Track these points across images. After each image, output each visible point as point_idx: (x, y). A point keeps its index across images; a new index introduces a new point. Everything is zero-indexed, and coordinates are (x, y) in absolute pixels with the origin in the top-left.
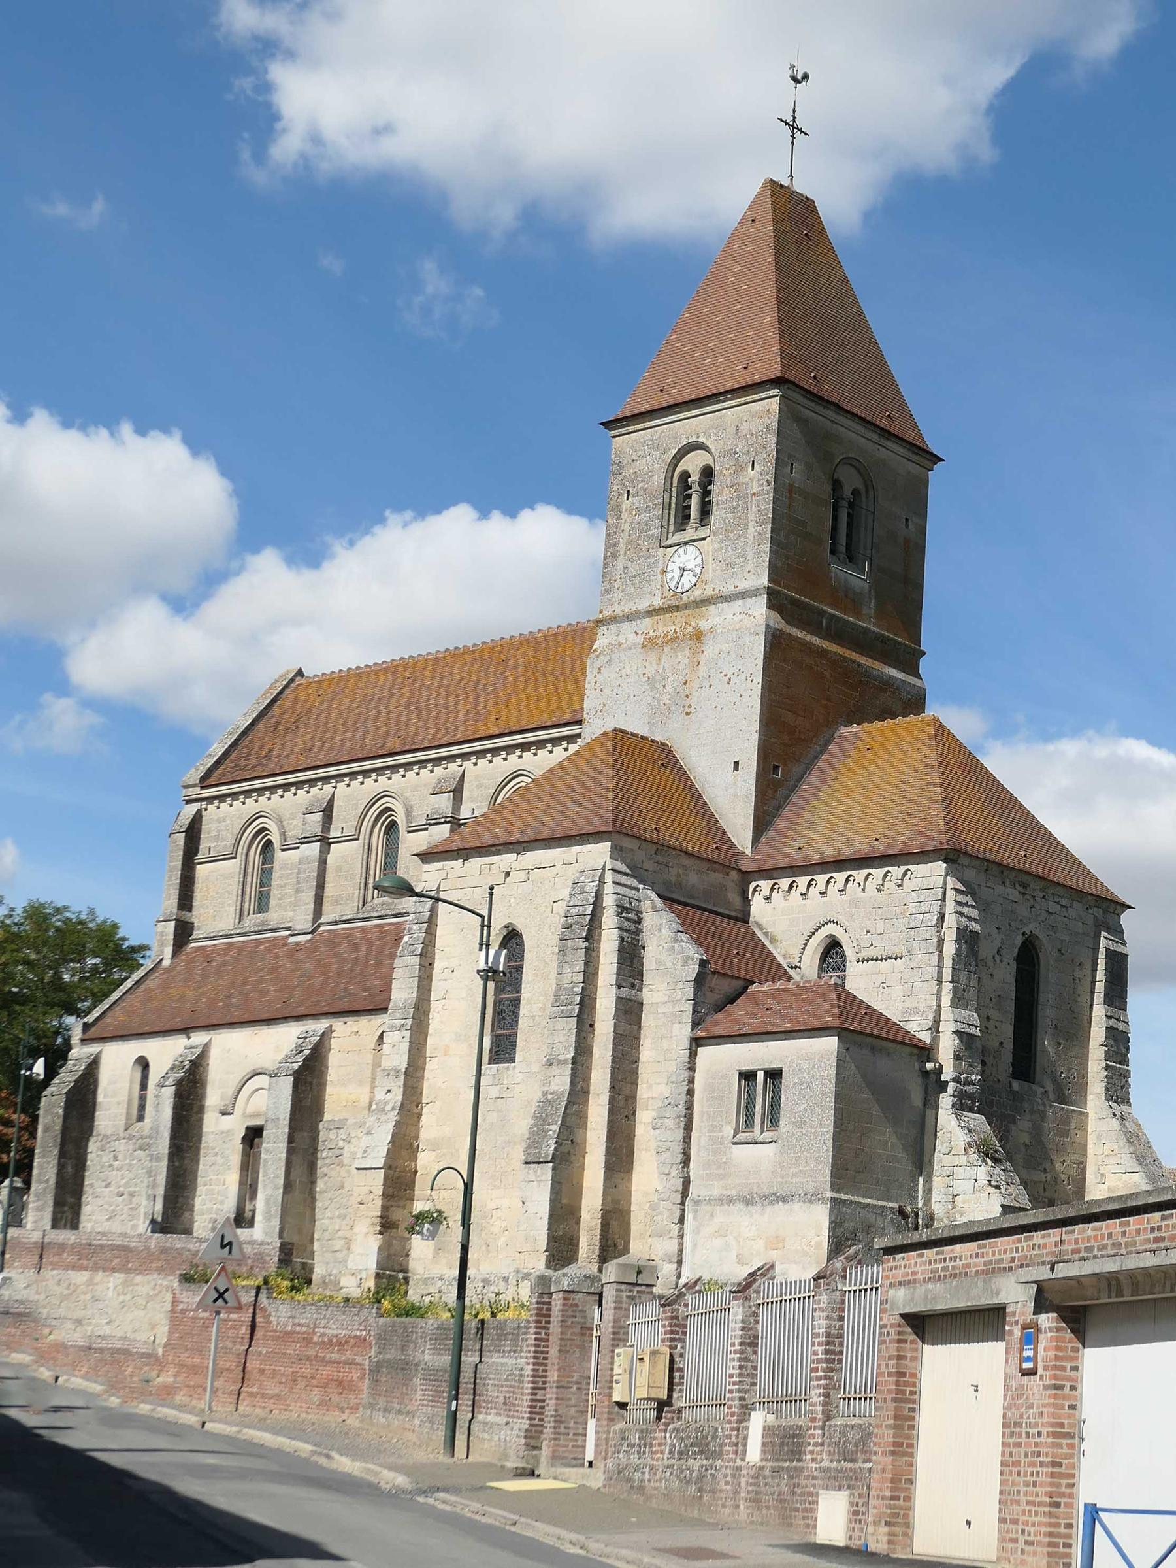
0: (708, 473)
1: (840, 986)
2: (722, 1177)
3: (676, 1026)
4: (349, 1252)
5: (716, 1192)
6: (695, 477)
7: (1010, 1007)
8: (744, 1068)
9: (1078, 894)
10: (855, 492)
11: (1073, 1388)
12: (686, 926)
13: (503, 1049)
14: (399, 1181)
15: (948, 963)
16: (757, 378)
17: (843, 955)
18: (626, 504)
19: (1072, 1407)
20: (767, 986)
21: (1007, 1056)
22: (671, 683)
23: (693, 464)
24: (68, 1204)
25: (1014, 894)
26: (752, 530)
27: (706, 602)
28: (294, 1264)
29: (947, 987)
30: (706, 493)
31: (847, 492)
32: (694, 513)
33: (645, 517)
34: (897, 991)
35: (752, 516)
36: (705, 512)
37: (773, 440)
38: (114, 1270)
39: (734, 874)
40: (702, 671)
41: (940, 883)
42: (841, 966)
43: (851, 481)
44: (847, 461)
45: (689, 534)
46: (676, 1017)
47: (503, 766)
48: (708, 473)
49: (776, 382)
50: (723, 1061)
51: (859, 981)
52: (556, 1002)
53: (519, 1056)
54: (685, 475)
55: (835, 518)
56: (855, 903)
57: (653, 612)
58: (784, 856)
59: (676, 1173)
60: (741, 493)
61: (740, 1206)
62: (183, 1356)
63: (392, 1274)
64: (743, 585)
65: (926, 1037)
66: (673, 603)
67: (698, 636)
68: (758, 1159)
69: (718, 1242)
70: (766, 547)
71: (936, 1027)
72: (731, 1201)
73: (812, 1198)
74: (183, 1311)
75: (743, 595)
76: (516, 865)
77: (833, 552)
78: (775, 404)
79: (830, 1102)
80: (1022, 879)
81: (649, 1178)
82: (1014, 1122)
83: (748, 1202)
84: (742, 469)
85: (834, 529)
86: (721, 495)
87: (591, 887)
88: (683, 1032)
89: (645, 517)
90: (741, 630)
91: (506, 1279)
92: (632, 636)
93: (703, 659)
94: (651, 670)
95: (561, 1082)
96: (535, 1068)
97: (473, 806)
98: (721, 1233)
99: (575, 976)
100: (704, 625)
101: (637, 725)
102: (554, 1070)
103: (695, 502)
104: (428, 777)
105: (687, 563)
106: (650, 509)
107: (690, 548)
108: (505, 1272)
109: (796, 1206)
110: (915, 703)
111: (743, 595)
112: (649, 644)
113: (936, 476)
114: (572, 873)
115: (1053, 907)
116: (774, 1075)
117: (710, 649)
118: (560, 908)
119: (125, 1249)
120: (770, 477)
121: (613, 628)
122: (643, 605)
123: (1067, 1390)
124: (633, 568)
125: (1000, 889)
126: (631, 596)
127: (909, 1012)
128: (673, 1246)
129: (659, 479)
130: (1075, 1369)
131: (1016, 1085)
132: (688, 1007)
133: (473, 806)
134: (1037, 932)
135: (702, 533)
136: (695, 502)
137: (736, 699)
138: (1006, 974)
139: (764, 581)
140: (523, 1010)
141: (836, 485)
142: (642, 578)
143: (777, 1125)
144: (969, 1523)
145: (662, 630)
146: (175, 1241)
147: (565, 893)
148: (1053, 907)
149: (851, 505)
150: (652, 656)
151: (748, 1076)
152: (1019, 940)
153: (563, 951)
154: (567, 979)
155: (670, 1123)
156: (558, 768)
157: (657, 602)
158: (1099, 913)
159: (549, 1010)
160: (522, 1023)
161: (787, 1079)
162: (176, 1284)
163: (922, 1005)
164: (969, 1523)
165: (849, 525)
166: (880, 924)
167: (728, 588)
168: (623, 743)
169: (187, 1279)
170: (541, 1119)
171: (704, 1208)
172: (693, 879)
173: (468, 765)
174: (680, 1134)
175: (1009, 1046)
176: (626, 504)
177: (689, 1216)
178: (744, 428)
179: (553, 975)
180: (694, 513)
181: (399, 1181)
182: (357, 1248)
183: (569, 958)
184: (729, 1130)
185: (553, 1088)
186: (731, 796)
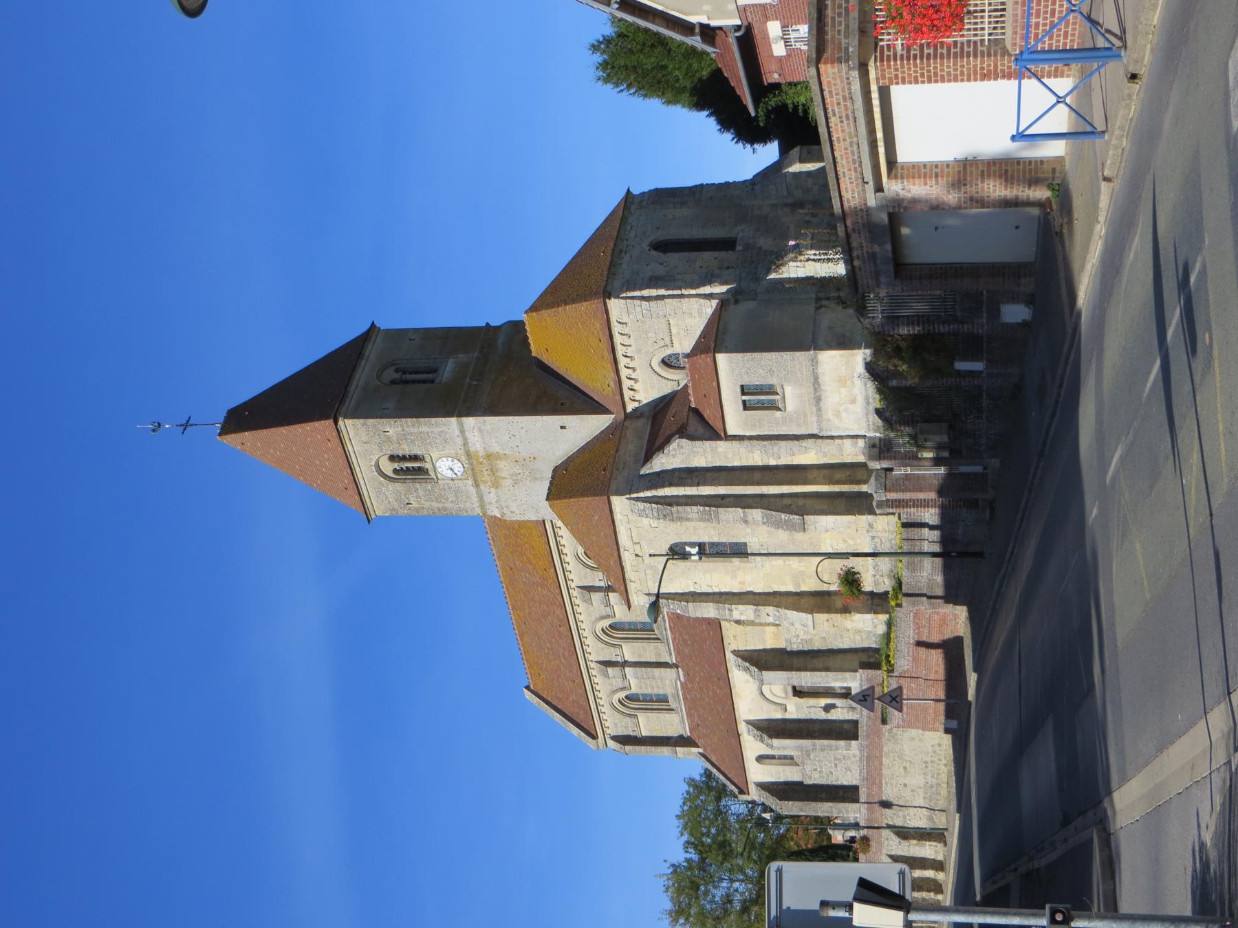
0: (393, 458)
1: (687, 356)
2: (805, 416)
3: (719, 450)
4: (862, 628)
5: (814, 419)
6: (396, 466)
7: (693, 255)
8: (741, 407)
9: (624, 220)
10: (397, 371)
11: (936, 167)
12: (661, 448)
13: (738, 551)
14: (819, 601)
15: (670, 292)
16: (335, 433)
17: (670, 356)
18: (415, 505)
19: (948, 166)
20: (692, 399)
21: (722, 255)
22: (517, 469)
23: (388, 467)
24: (847, 794)
25: (626, 258)
26: (424, 429)
27: (468, 454)
28: (870, 659)
29: (685, 292)
30: (403, 458)
31: (397, 376)
32: (416, 465)
33: (421, 492)
34: (689, 321)
35: (416, 430)
36: (415, 458)
37: (370, 421)
38: (881, 764)
39: (626, 424)
40: (507, 452)
41: (623, 301)
42: (676, 356)
43: (390, 374)
44: (379, 377)
45: (428, 466)
46: (713, 450)
47: (572, 565)
48: (393, 458)
49: (336, 423)
50: (735, 420)
51: (684, 344)
52: (710, 520)
53: (743, 540)
54: (395, 471)
55: (413, 382)
56: (639, 351)
57: (477, 485)
58: (614, 395)
59: (805, 443)
60: (403, 437)
61: (822, 404)
62: (930, 719)
63: (877, 602)
64: (457, 432)
65: (714, 303)
66: (470, 472)
67: (489, 456)
68: (792, 396)
69: (843, 415)
70: (433, 420)
71: (710, 296)
72: (819, 410)
73: (814, 362)
74: (903, 721)
75: (462, 432)
76: (631, 551)
77: (432, 381)
78: (349, 422)
79: (757, 355)
80: (617, 253)
81: (808, 456)
82: (760, 248)
83: (818, 400)
84: (389, 438)
85: (419, 382)
86: (406, 449)
87: (641, 505)
88: (721, 446)
89: (421, 492)
90: (484, 432)
91: (873, 538)
92: (492, 495)
93: (501, 452)
94: (509, 482)
95: (756, 514)
96: (749, 530)
97: (598, 579)
98: (838, 414)
99: (693, 511)
100: (482, 453)
101: (545, 486)
102: (750, 519)
103: (410, 465)
104: (582, 608)
105: (446, 466)
106: (416, 490)
107: (437, 465)
108: (869, 539)
109: (820, 370)
110: (517, 328)
111: (462, 432)
112: (496, 485)
113: (383, 325)
114: (632, 517)
115: (632, 234)
116: (744, 390)
117: (496, 448)
118: (654, 523)
119: (868, 758)
120: (392, 421)
121: (488, 507)
122: (473, 490)
123: (938, 170)
124: (452, 497)
125: (624, 266)
126: (468, 497)
127: (700, 314)
128: (848, 442)
129: (398, 486)
130: (925, 166)
131: (739, 248)
132: (708, 444)
133: (598, 579)
134: (648, 242)
135: (428, 459)
136: (410, 465)
137: (523, 431)
138: (674, 259)
139: (454, 420)
140: (716, 540)
141: (393, 382)
142: (457, 492)
143: (771, 386)
144: (1017, 227)
145: (486, 478)
146: (863, 730)
147: (645, 521)
148: (632, 234)
149: (404, 373)
150: (503, 483)
151: (746, 406)
152: (654, 253)
153: (680, 519)
154: (695, 516)
155: (776, 450)
156: (572, 531)
157: (470, 482)
158: (633, 207)
159: (715, 524)
160: (723, 540)
161: (746, 381)
162: (888, 727)
163: (696, 306)
164: (1017, 227)
165: (416, 373)
166: (650, 335)
167: (460, 441)
168: (554, 494)
169: (884, 722)
170: (778, 525)
171: (824, 425)
172: (631, 447)
173: (573, 585)
174: (783, 443)
175: (716, 254)
176: (415, 505)
177: (829, 434)
178: (364, 438)
179: (693, 524)
180: (416, 465)
181: (819, 601)
182: (861, 626)
183: (683, 515)
184: (778, 414)
185: (760, 519)
186: (581, 430)
